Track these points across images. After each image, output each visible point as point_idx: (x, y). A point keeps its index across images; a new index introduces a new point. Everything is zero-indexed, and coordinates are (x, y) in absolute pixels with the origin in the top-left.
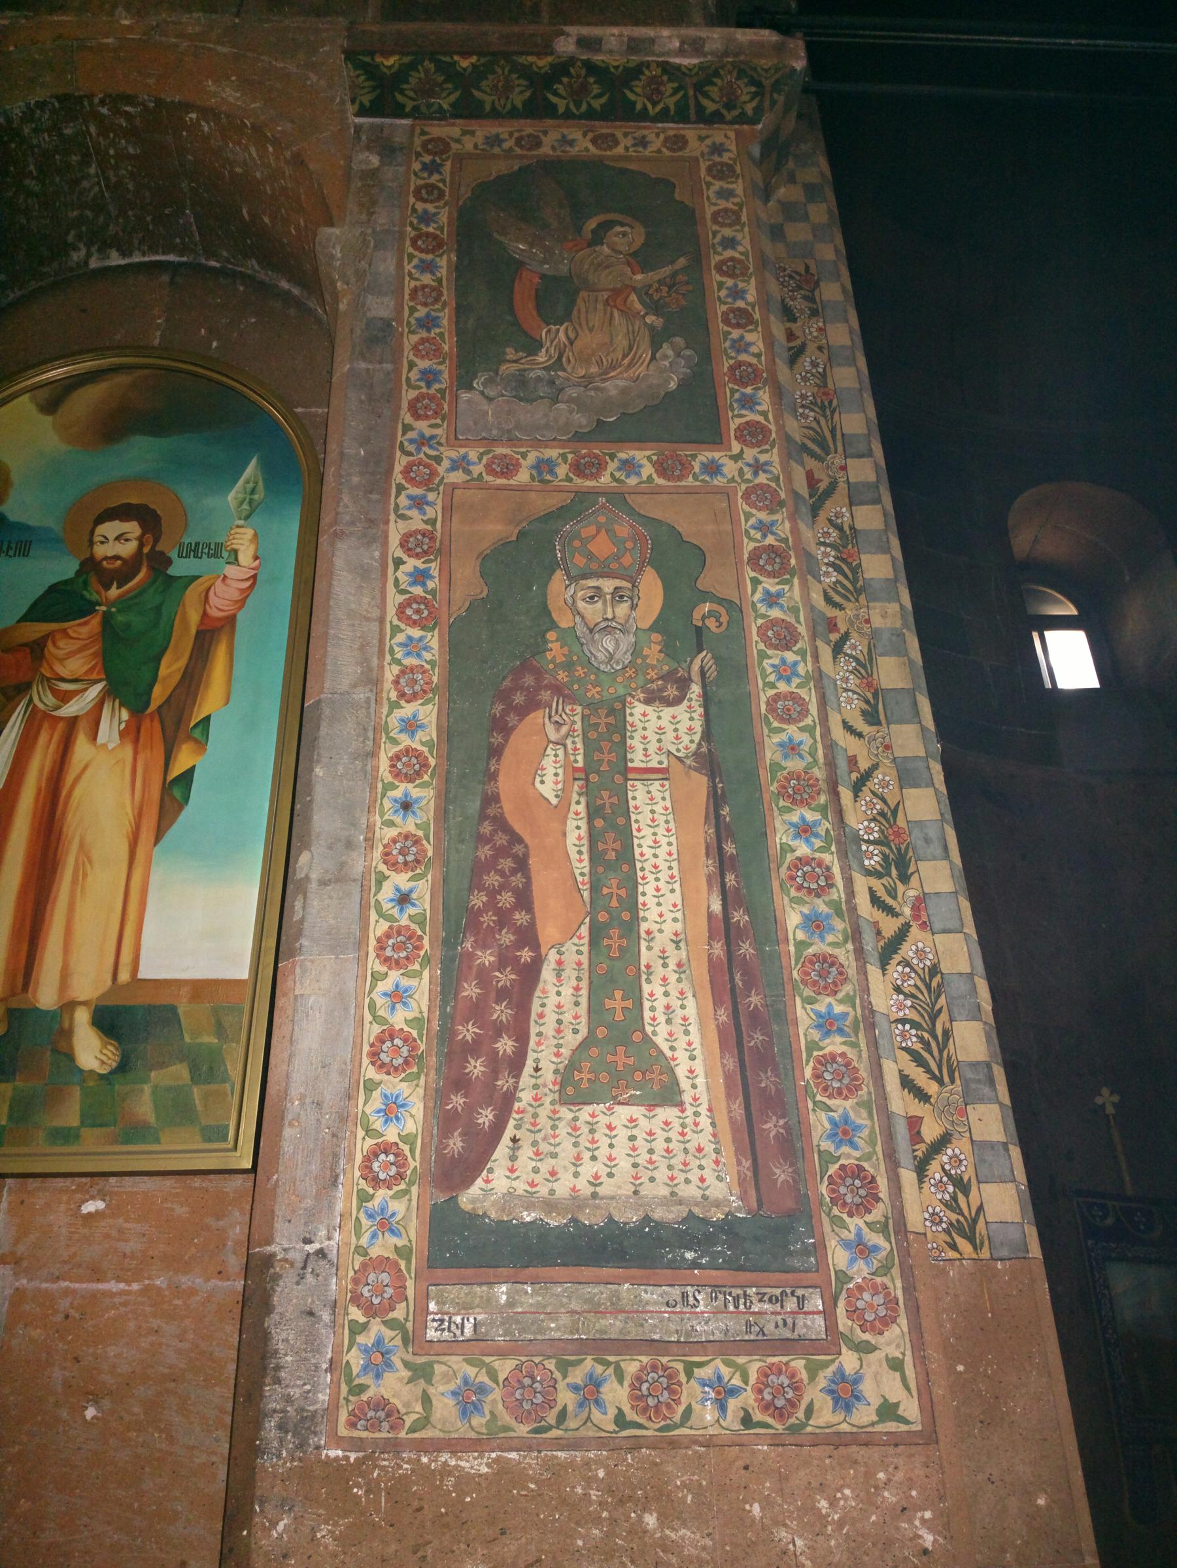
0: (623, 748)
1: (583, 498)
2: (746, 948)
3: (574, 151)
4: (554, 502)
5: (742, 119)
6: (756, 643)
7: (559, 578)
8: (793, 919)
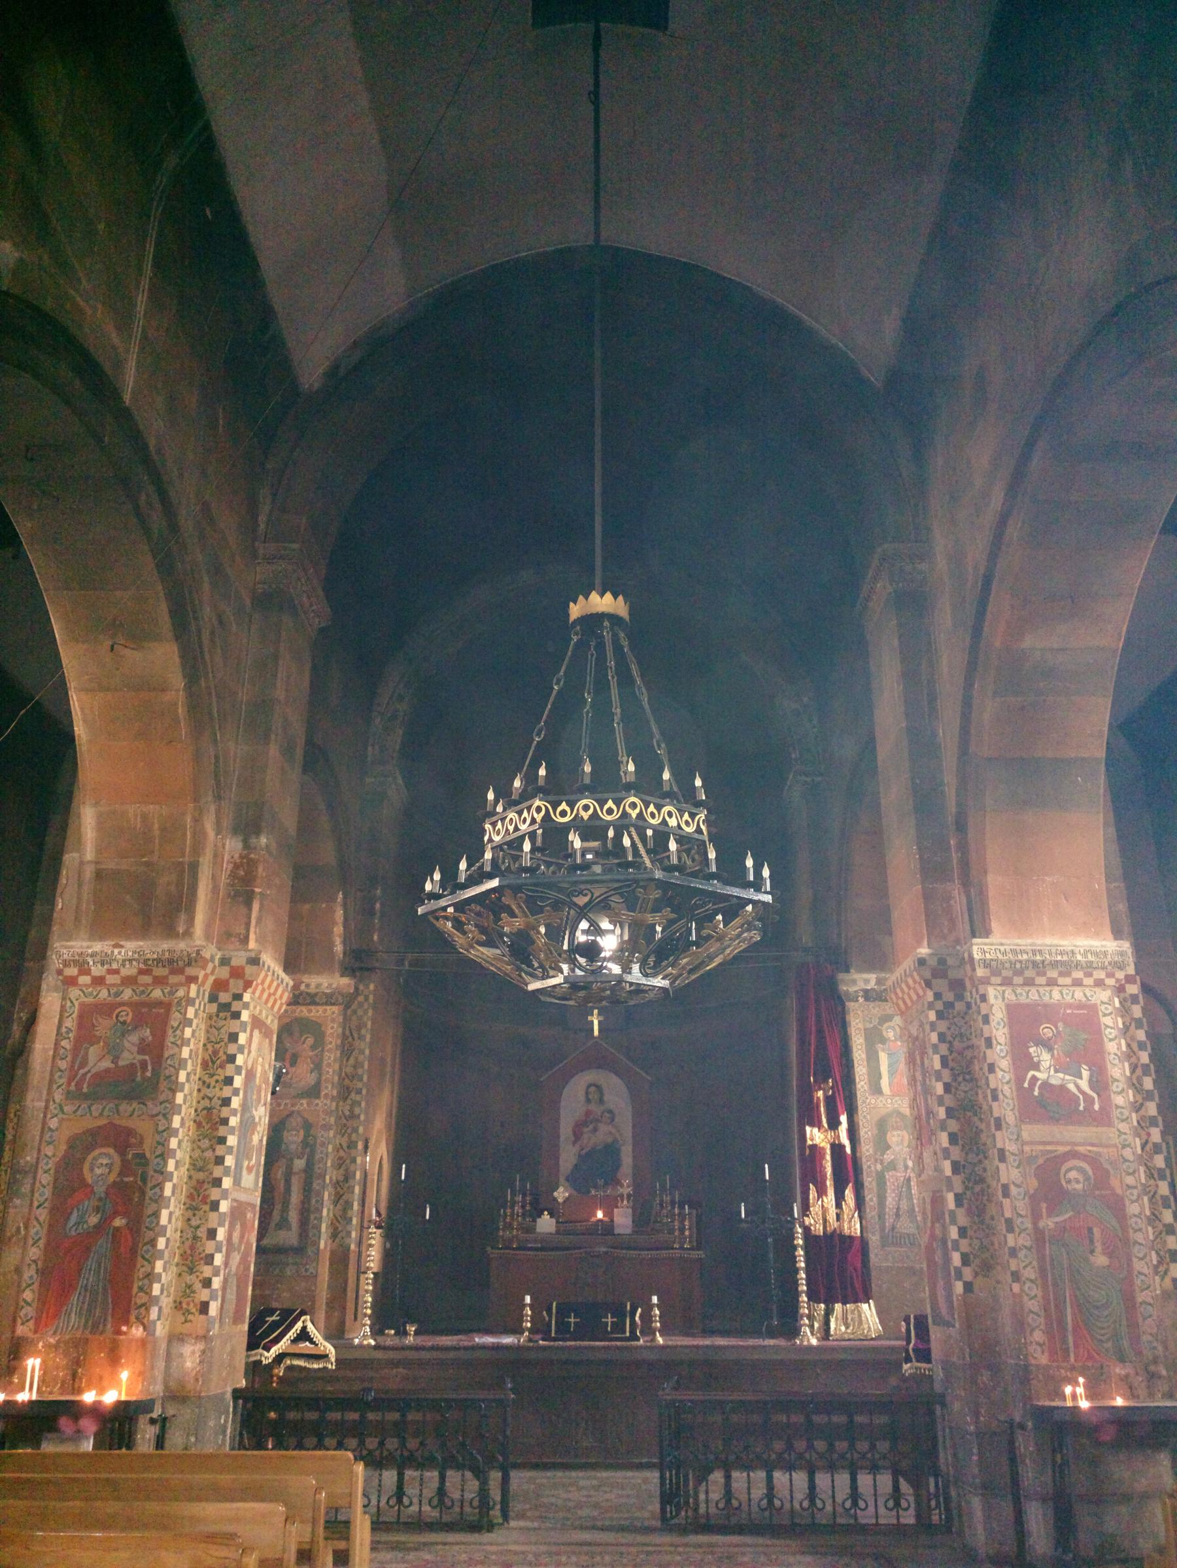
0: (292, 1169)
1: (293, 1112)
2: (306, 1206)
3: (303, 1014)
4: (288, 1113)
5: (340, 1004)
6: (318, 1146)
7: (285, 1133)
8: (314, 1201)
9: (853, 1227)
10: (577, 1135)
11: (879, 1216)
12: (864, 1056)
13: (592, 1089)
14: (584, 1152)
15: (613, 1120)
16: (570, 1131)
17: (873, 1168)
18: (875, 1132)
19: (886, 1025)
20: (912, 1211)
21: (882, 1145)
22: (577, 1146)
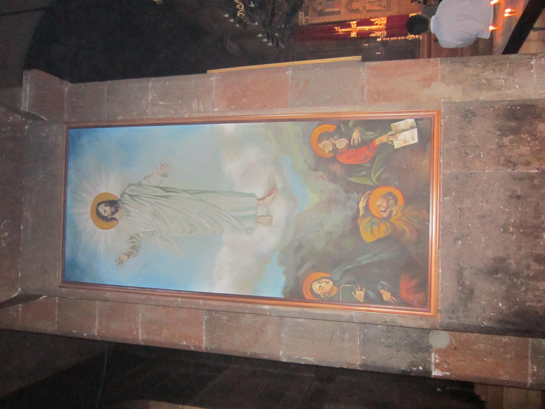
9: (384, 21)
17: (364, 14)
21: (357, 11)
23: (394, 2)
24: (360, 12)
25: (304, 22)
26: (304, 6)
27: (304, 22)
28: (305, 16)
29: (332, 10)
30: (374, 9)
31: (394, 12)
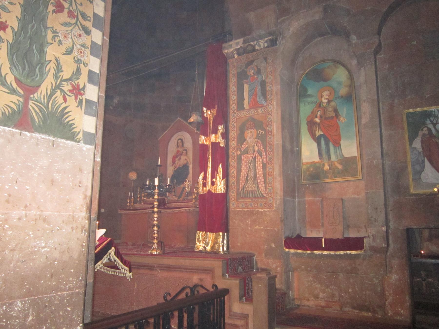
10: (174, 162)
11: (237, 182)
12: (235, 89)
13: (180, 141)
14: (175, 169)
15: (187, 153)
16: (171, 160)
18: (239, 132)
19: (249, 67)
20: (255, 178)
21: (241, 139)
22: (173, 167)
23: (251, 205)
24: (239, 145)
25: (226, 51)
26: (252, 43)
27: (226, 51)
28: (237, 50)
29: (246, 94)
30: (242, 169)
31: (233, 205)
